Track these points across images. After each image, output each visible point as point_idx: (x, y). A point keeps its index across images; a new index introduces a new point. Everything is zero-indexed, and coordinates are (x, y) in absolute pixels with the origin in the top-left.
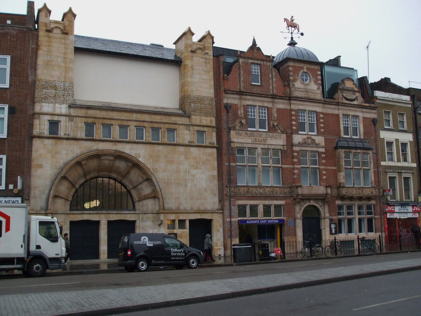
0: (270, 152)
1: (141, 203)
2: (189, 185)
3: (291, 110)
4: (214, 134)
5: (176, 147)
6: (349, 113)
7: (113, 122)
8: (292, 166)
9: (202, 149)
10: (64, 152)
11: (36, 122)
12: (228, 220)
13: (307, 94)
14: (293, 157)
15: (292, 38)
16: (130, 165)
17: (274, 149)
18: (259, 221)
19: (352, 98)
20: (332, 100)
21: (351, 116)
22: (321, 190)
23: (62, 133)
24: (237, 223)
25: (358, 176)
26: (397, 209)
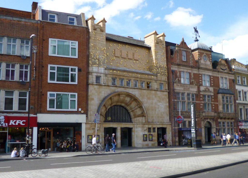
0: (191, 95)
1: (135, 119)
2: (157, 110)
3: (200, 74)
4: (167, 85)
5: (151, 91)
6: (223, 76)
7: (124, 78)
8: (200, 102)
9: (162, 92)
10: (103, 92)
11: (90, 76)
12: (174, 128)
13: (206, 67)
14: (201, 97)
15: (196, 38)
16: (132, 99)
17: (192, 93)
19: (224, 69)
20: (216, 70)
21: (224, 78)
22: (213, 114)
23: (102, 82)
24: (177, 130)
25: (228, 108)
26: (243, 124)
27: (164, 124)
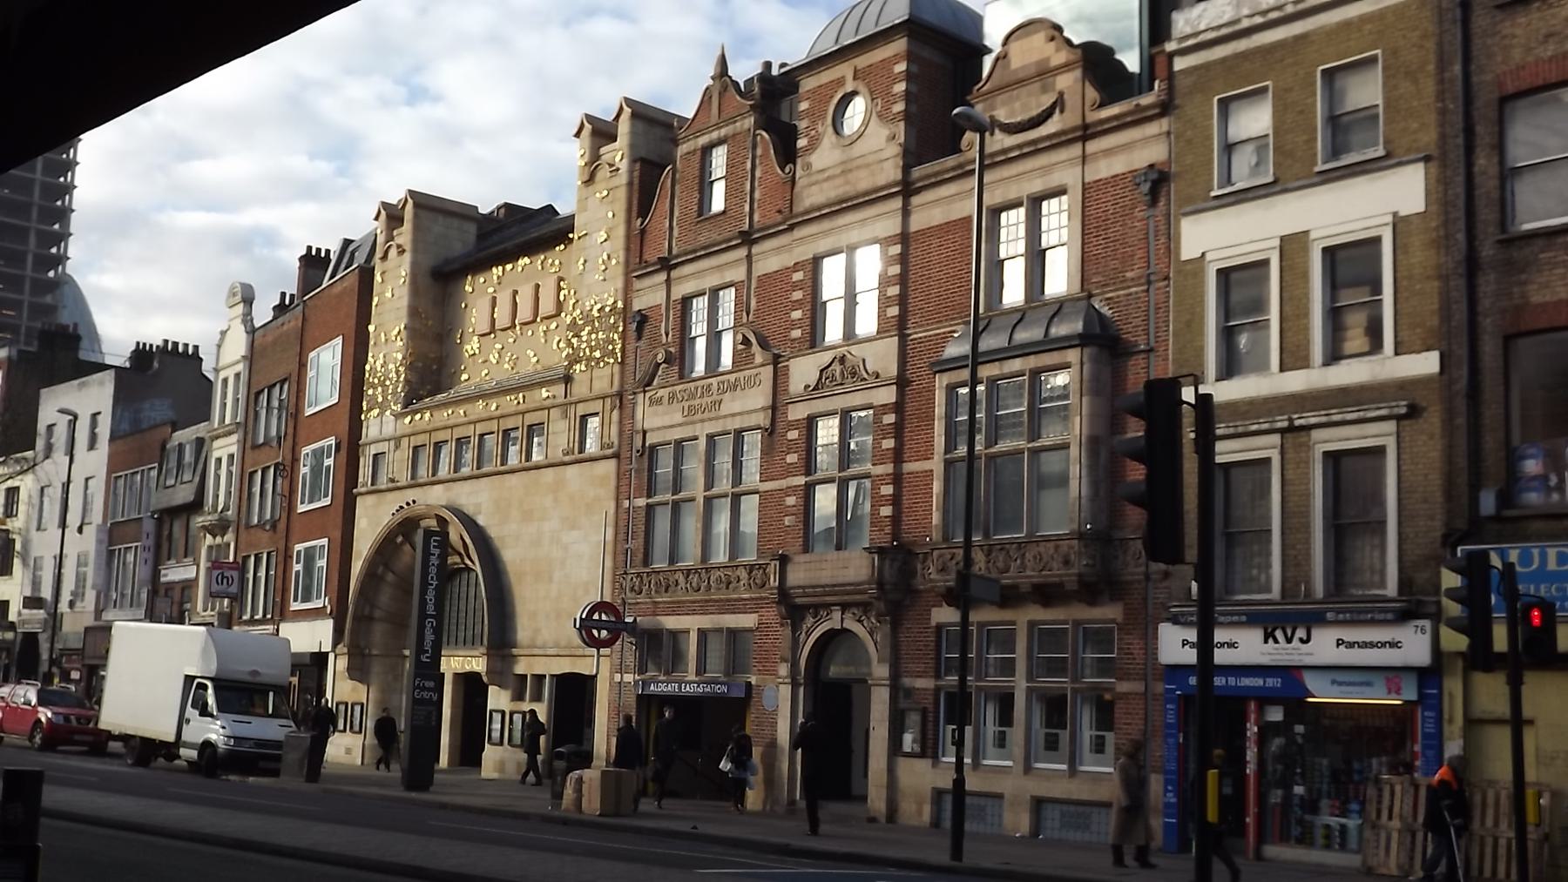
2: (557, 575)
13: (847, 183)
18: (680, 688)
27: (577, 653)
